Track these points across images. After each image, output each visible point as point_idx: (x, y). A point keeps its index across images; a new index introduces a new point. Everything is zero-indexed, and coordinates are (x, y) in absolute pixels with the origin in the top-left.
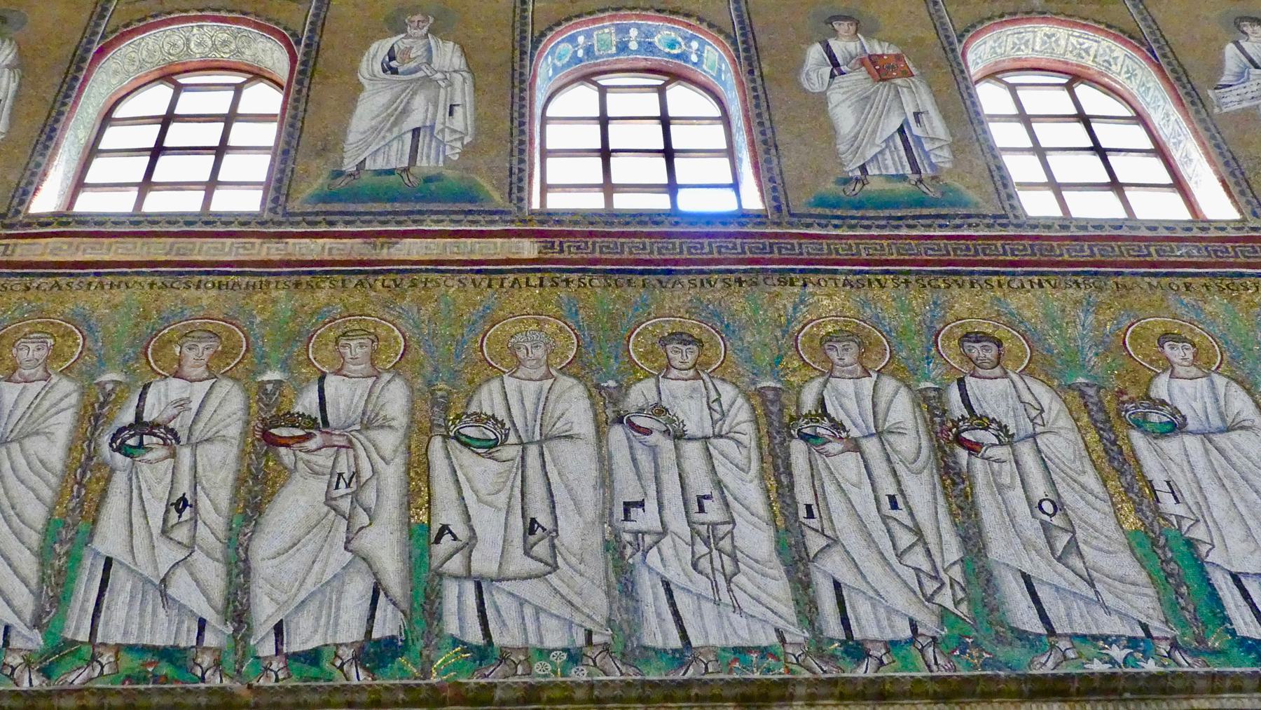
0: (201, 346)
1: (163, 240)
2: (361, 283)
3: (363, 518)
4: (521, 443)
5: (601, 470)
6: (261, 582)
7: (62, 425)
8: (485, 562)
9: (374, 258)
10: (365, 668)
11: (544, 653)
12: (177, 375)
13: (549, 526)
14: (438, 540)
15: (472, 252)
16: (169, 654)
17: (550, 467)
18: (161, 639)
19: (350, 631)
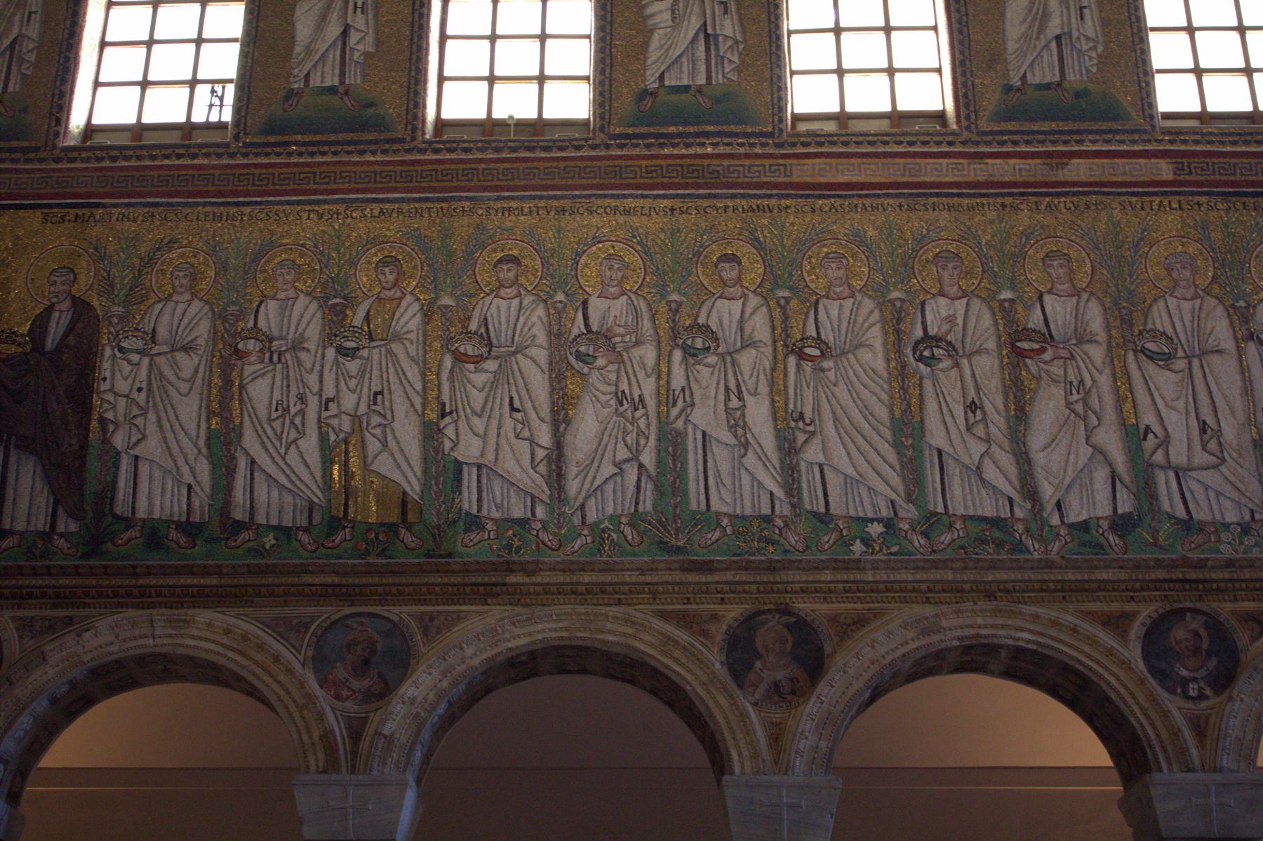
0: (950, 265)
1: (897, 160)
2: (1049, 206)
3: (1093, 420)
4: (1187, 357)
5: (1244, 380)
6: (1039, 470)
7: (875, 335)
8: (1178, 454)
9: (1054, 179)
10: (1119, 536)
11: (1226, 526)
12: (941, 293)
13: (1215, 427)
14: (1145, 439)
15: (1124, 174)
16: (995, 522)
17: (1210, 379)
18: (989, 512)
19: (1103, 509)
